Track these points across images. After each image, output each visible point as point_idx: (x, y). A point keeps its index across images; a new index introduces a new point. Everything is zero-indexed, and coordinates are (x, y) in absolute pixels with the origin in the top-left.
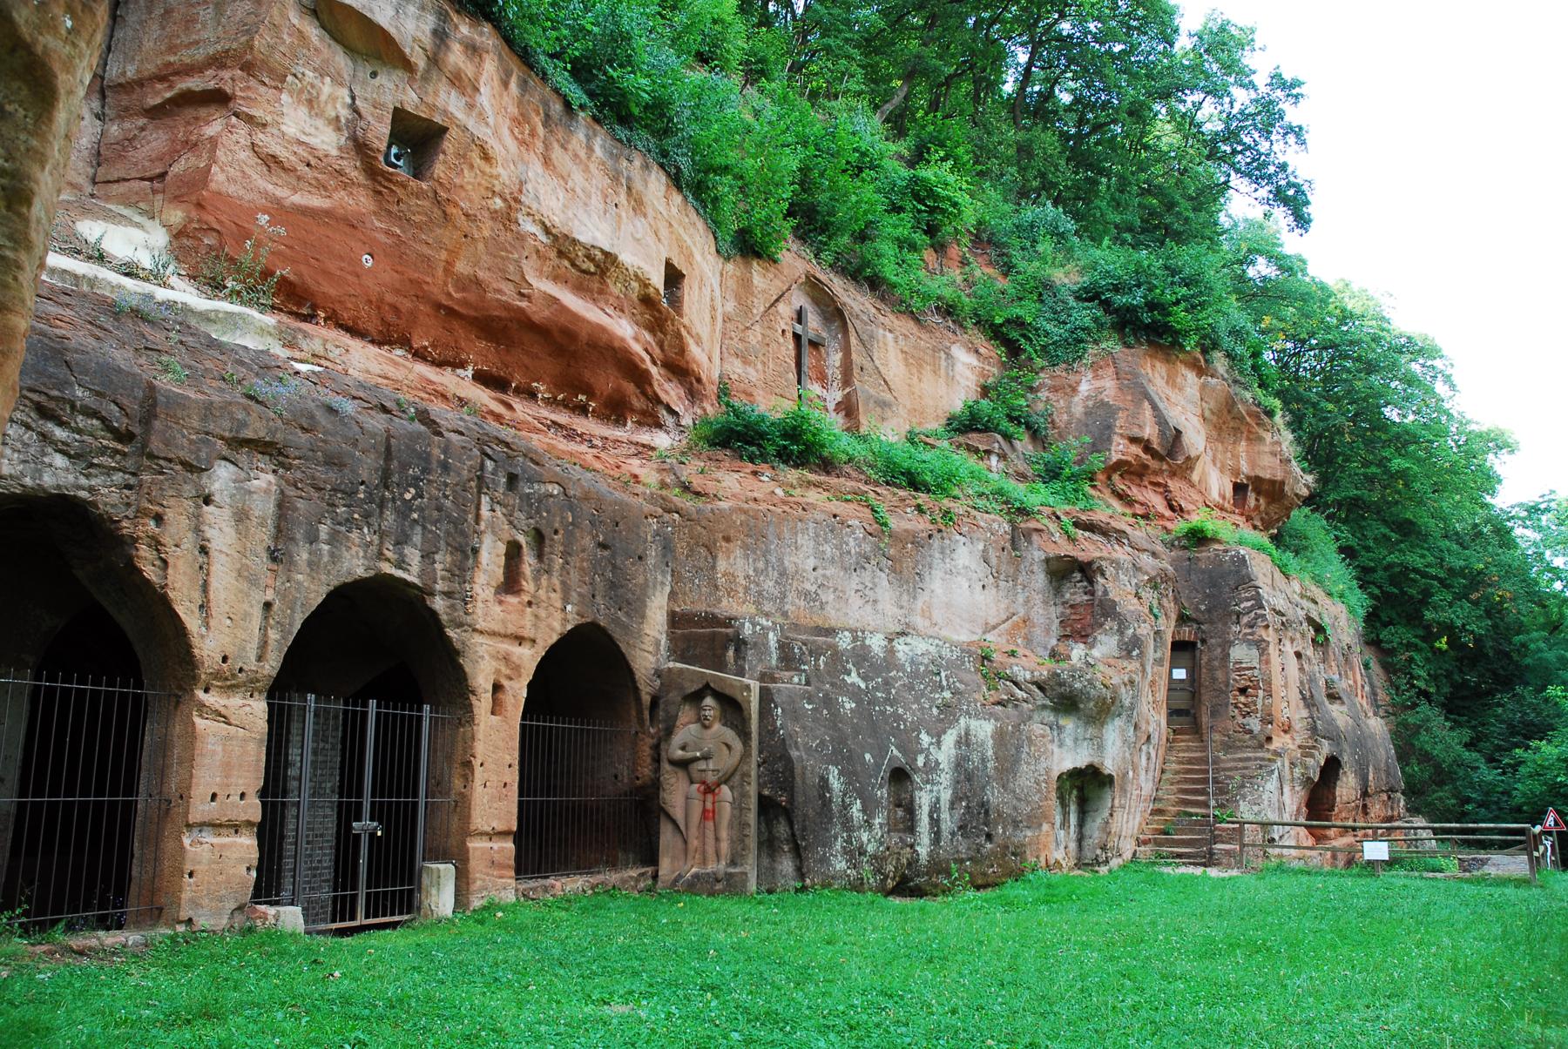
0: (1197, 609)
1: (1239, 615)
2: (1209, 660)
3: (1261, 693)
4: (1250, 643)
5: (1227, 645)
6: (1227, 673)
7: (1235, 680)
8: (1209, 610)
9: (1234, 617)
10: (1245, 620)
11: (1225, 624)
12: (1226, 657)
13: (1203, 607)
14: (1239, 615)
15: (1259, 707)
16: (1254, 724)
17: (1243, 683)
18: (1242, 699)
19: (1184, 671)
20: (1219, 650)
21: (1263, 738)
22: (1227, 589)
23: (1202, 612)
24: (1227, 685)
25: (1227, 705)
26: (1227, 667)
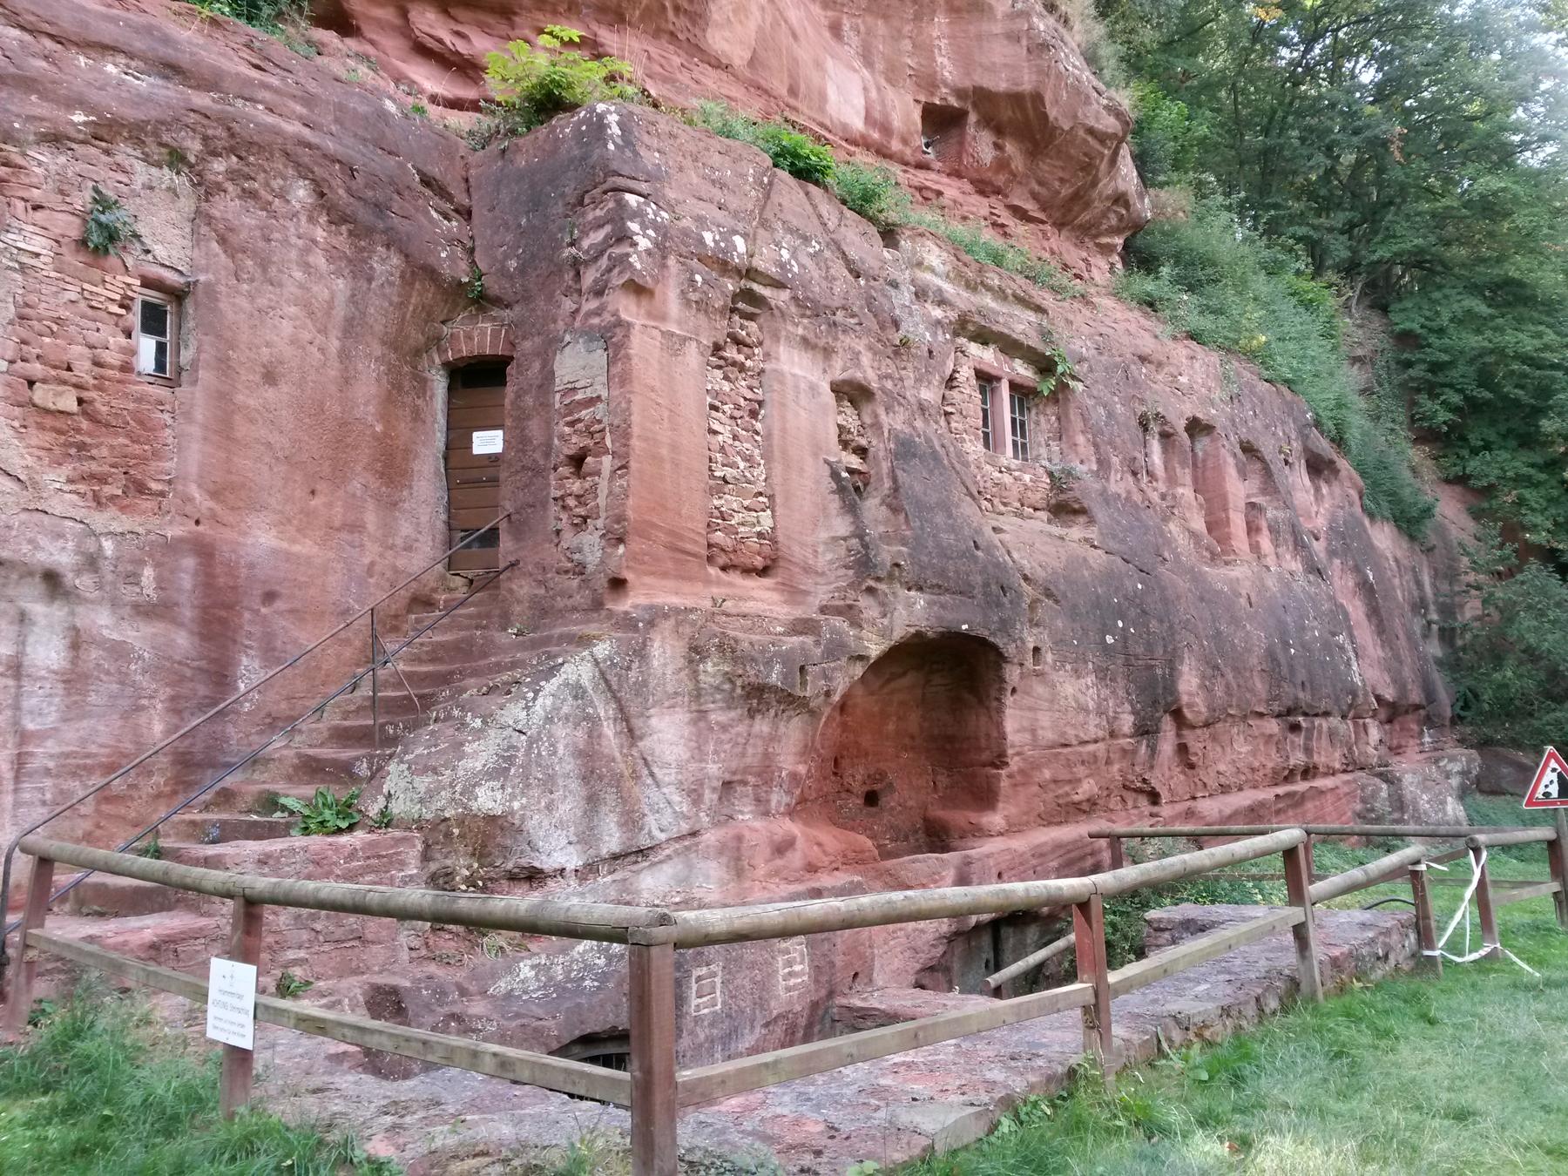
0: (503, 272)
1: (576, 265)
2: (518, 396)
3: (607, 461)
4: (590, 334)
5: (552, 345)
6: (548, 424)
7: (562, 437)
8: (522, 270)
9: (569, 276)
10: (589, 277)
11: (550, 298)
12: (548, 376)
13: (513, 264)
14: (576, 265)
15: (602, 501)
16: (590, 546)
17: (578, 442)
18: (576, 486)
19: (498, 435)
20: (537, 365)
21: (601, 582)
22: (560, 208)
23: (511, 277)
24: (548, 450)
25: (544, 505)
26: (546, 406)
